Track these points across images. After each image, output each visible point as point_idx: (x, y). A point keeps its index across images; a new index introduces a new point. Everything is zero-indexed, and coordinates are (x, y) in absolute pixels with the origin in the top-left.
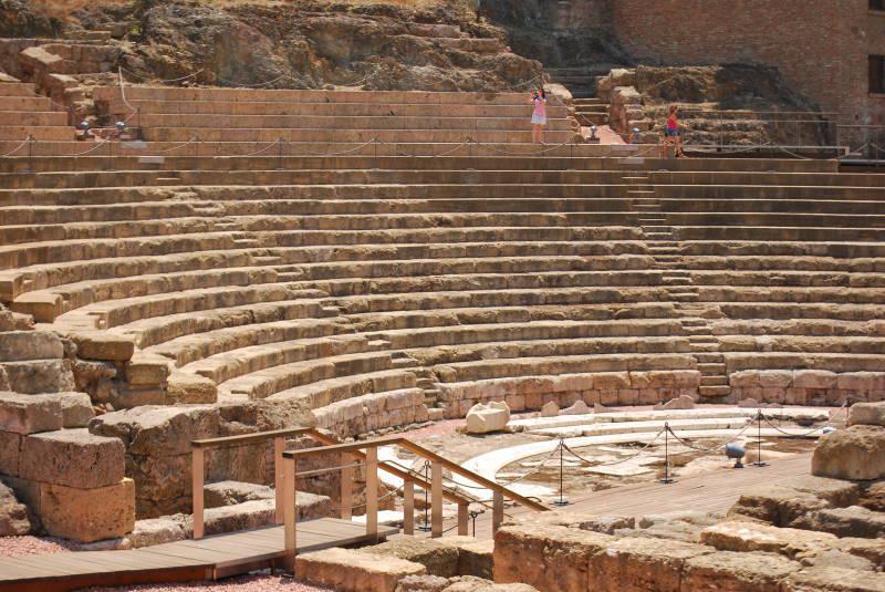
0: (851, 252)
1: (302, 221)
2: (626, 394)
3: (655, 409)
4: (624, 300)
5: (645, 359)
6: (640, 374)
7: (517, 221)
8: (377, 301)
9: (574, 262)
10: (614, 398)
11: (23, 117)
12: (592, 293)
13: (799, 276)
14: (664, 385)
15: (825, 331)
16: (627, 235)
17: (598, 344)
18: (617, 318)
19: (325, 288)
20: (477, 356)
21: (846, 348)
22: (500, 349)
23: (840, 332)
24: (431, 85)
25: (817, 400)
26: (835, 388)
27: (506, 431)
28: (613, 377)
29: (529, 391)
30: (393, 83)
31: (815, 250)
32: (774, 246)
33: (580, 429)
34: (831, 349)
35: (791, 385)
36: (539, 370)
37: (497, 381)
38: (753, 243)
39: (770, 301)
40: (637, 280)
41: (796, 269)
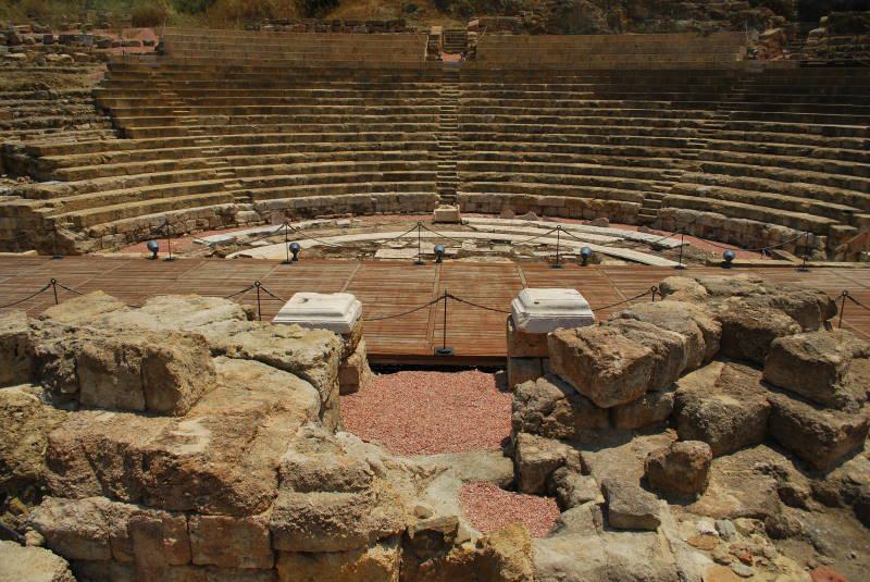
0: (839, 132)
2: (587, 213)
3: (583, 224)
4: (648, 155)
6: (599, 201)
7: (639, 105)
8: (480, 145)
9: (641, 130)
10: (579, 214)
11: (395, 50)
14: (613, 210)
15: (753, 187)
16: (699, 116)
17: (592, 180)
18: (630, 166)
19: (460, 136)
20: (506, 179)
21: (752, 201)
22: (523, 177)
23: (764, 189)
24: (686, 30)
25: (710, 236)
26: (722, 228)
27: (456, 223)
29: (520, 202)
30: (668, 28)
31: (814, 130)
33: (492, 227)
34: (738, 199)
35: (695, 221)
36: (534, 191)
37: (495, 194)
38: (772, 123)
39: (744, 163)
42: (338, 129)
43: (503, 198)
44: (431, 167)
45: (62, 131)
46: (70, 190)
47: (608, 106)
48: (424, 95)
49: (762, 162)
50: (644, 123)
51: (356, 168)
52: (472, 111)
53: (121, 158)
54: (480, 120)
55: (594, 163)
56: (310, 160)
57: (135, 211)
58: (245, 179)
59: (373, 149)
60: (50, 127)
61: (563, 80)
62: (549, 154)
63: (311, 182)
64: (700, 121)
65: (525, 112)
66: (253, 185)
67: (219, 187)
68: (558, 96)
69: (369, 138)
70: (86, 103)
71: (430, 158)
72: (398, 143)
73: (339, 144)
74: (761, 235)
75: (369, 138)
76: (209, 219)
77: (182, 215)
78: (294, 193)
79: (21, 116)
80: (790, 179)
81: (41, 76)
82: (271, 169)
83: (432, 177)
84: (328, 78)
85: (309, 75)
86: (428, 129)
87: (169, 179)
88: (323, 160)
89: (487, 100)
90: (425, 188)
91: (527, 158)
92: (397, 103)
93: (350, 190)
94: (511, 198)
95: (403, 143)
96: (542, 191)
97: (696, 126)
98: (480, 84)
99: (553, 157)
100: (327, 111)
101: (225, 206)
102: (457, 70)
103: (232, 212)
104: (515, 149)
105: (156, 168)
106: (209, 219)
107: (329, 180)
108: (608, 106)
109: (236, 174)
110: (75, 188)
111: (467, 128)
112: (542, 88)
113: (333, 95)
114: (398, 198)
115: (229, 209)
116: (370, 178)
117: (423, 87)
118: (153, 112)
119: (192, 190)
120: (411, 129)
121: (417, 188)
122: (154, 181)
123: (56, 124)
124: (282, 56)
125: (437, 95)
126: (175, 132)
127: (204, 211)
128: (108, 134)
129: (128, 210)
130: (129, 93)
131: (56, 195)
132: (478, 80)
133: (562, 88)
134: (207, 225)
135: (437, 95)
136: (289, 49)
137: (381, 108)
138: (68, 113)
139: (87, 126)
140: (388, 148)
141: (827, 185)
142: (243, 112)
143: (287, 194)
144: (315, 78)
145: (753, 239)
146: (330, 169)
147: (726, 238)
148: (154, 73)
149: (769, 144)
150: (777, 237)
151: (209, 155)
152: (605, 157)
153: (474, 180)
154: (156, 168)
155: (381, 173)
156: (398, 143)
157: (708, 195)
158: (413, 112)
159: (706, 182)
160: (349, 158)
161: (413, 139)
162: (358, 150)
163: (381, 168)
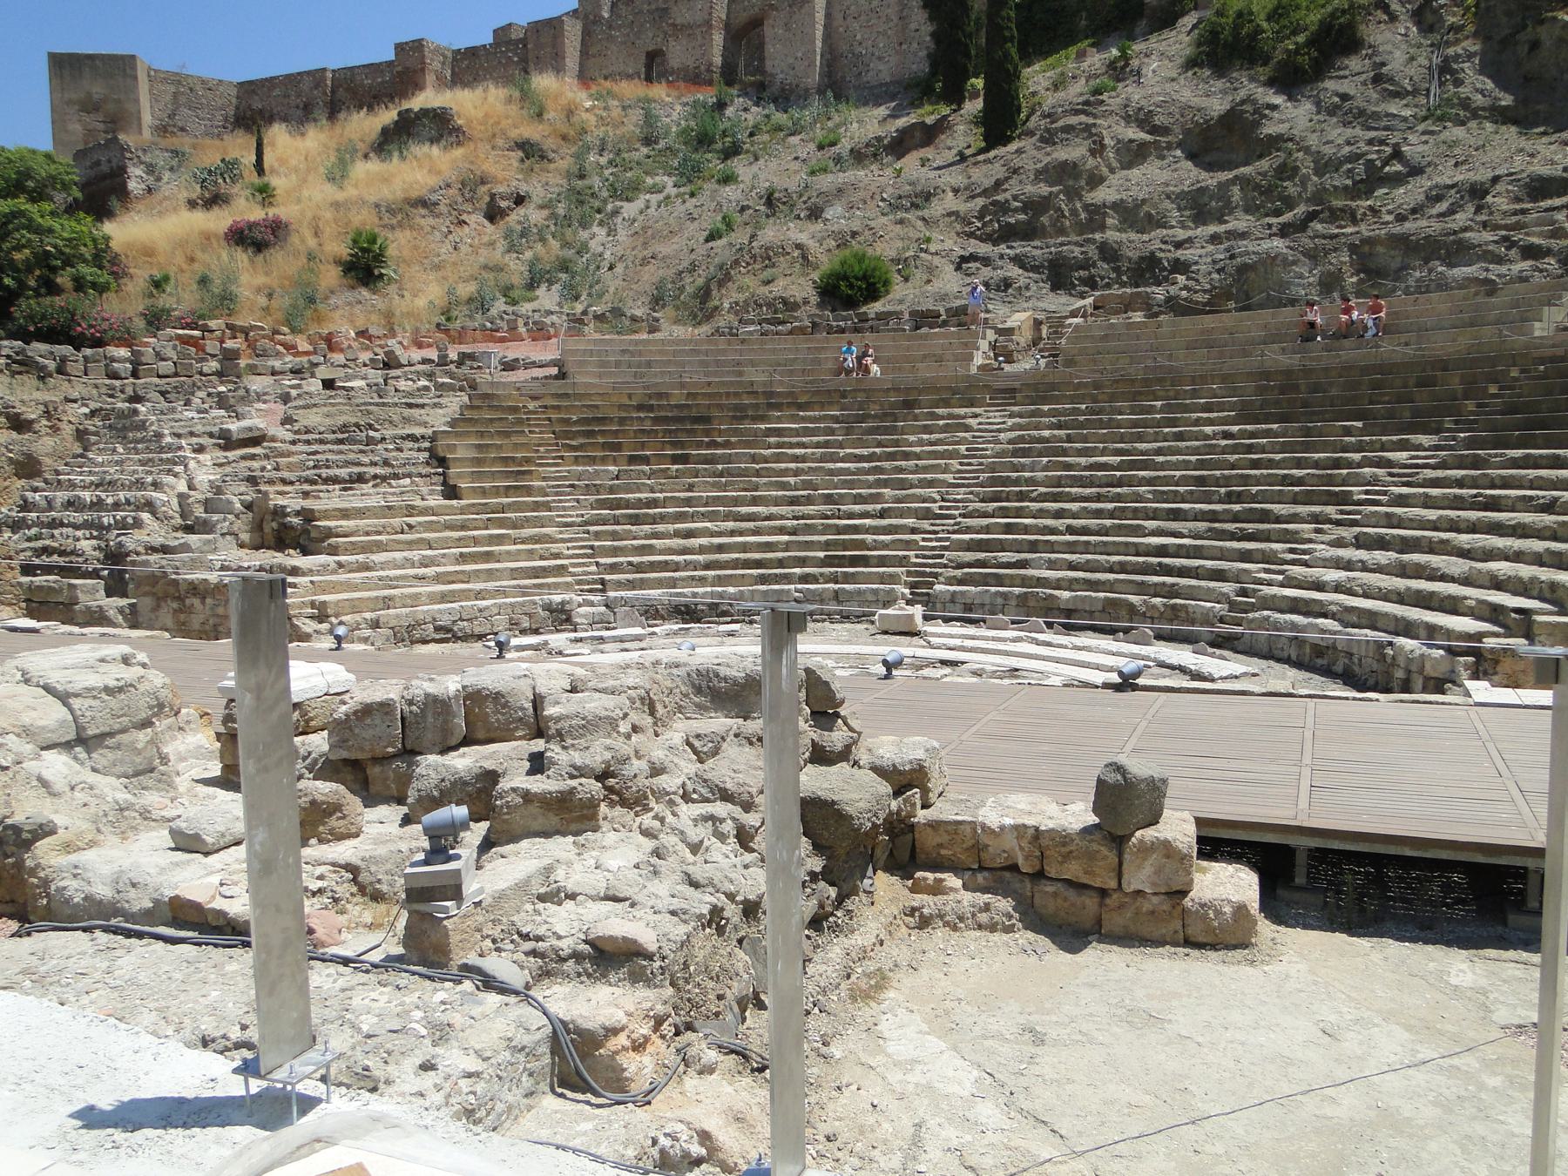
1: (1068, 435)
4: (1278, 520)
5: (1173, 585)
6: (1157, 601)
8: (1001, 508)
9: (1285, 476)
11: (925, 356)
12: (1245, 510)
13: (1500, 497)
17: (1160, 564)
28: (1126, 600)
32: (1541, 456)
36: (1058, 584)
37: (993, 589)
40: (1324, 498)
41: (1531, 488)
42: (784, 486)
43: (1004, 595)
44: (908, 545)
45: (367, 488)
46: (333, 566)
47: (1252, 435)
48: (946, 429)
49: (1463, 526)
50: (1299, 464)
51: (787, 546)
52: (1015, 453)
53: (430, 527)
54: (1022, 468)
55: (1182, 536)
56: (720, 534)
57: (415, 600)
58: (602, 561)
59: (827, 517)
60: (345, 481)
61: (1195, 394)
62: (1108, 522)
63: (707, 567)
64: (1401, 456)
65: (1103, 453)
66: (614, 568)
67: (561, 570)
68: (1173, 423)
69: (829, 499)
70: (419, 450)
71: (914, 531)
72: (869, 507)
73: (774, 510)
74: (1384, 656)
75: (829, 499)
76: (530, 615)
77: (487, 608)
78: (673, 583)
79: (315, 467)
80: (1490, 555)
81: (369, 413)
82: (651, 546)
83: (902, 562)
84: (801, 407)
85: (771, 402)
86: (931, 484)
87: (488, 557)
88: (741, 534)
89: (1046, 433)
90: (882, 579)
91: (1071, 530)
92: (896, 444)
93: (763, 580)
94: (1018, 596)
95: (879, 507)
96: (1070, 585)
97: (1389, 464)
98: (1046, 408)
99: (1114, 526)
100: (778, 458)
101: (557, 598)
102: (1017, 384)
103: (567, 607)
104: (1059, 514)
105: (476, 541)
106: (530, 615)
107: (736, 564)
108: (1252, 435)
109: (595, 552)
110: (340, 565)
111: (993, 482)
112: (1151, 410)
113: (797, 433)
114: (836, 592)
115: (563, 603)
116: (802, 562)
117: (951, 416)
118: (506, 461)
119: (515, 573)
120: (903, 485)
121: (869, 579)
122: (463, 558)
123: (361, 479)
124: (740, 374)
125: (967, 428)
126: (528, 491)
127: (522, 604)
128: (432, 492)
129: (404, 596)
130: (481, 434)
131: (310, 572)
132: (1044, 401)
133: (1187, 409)
134: (526, 625)
135: (967, 428)
136: (753, 363)
137: (865, 452)
138: (386, 463)
139: (408, 481)
140: (851, 516)
141: (1542, 565)
142: (646, 460)
143: (659, 583)
144: (778, 407)
145: (1375, 666)
146: (744, 548)
147: (1339, 668)
148: (532, 405)
149: (1488, 492)
150: (1401, 661)
151: (567, 525)
152: (1199, 524)
153: (970, 565)
154: (476, 541)
155: (821, 554)
156: (869, 507)
157: (1338, 588)
158: (918, 457)
159: (1348, 566)
160: (782, 531)
161: (899, 501)
162: (803, 518)
163: (827, 546)
